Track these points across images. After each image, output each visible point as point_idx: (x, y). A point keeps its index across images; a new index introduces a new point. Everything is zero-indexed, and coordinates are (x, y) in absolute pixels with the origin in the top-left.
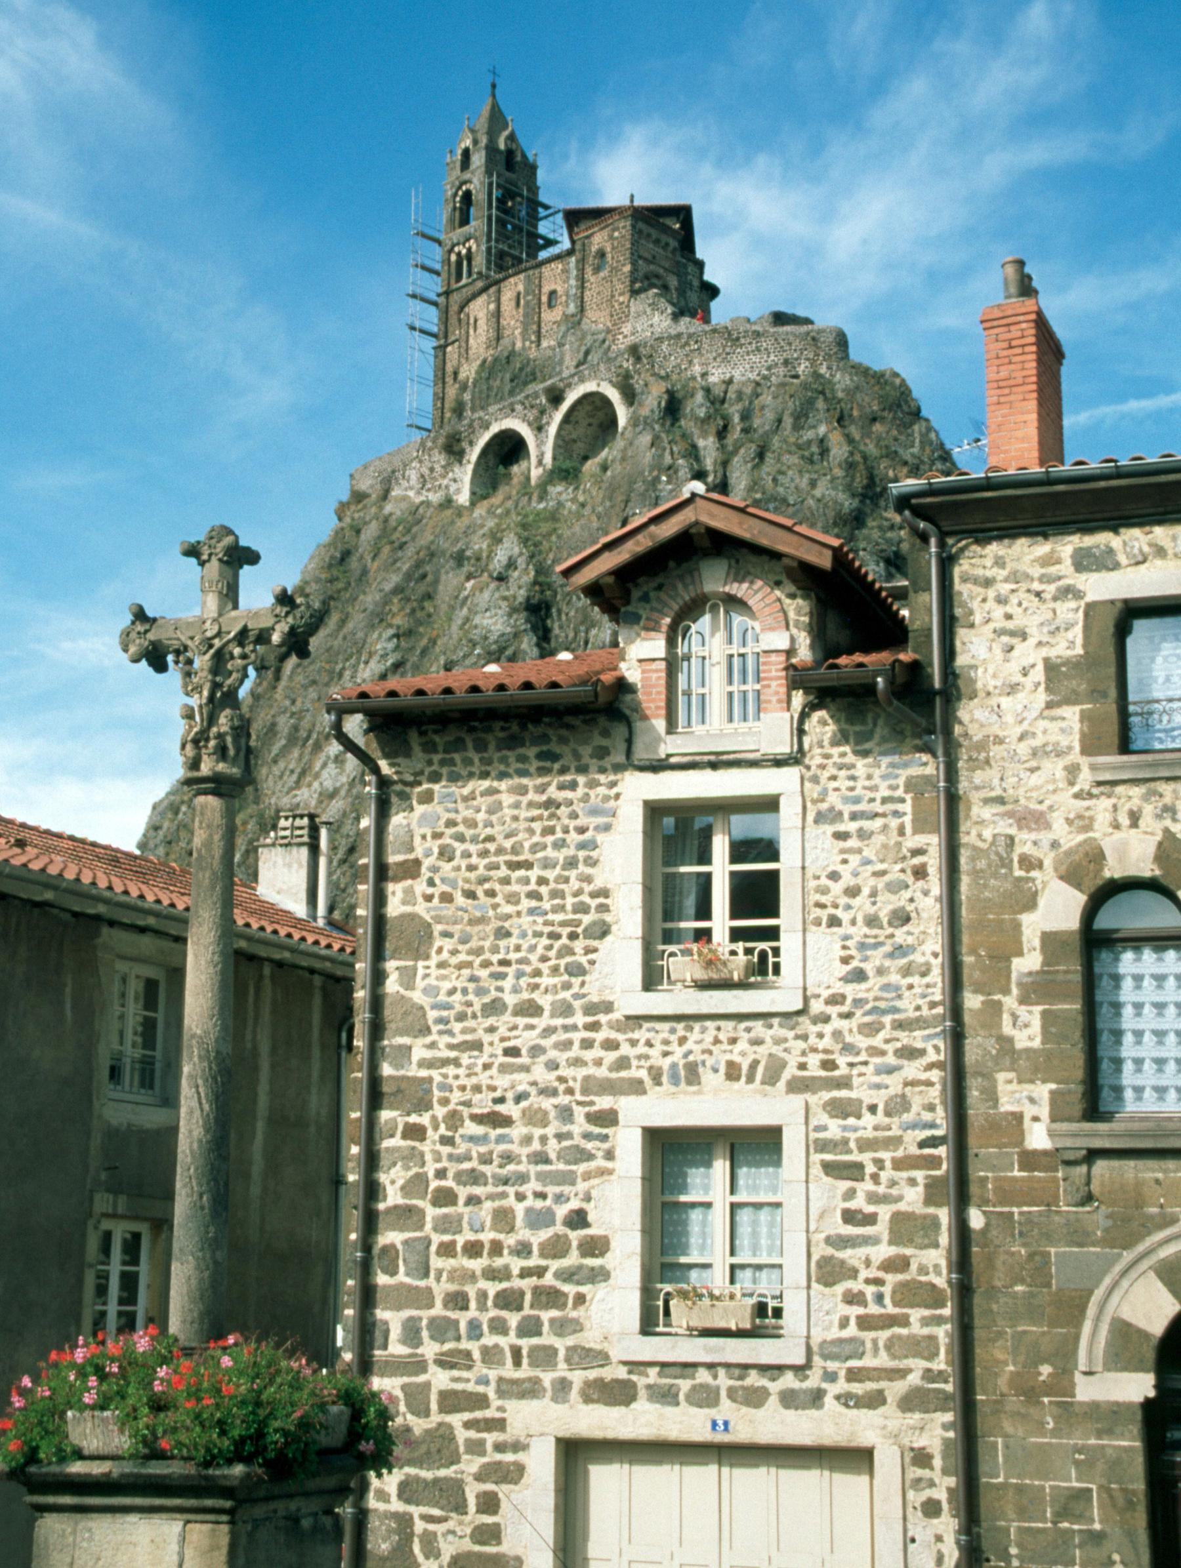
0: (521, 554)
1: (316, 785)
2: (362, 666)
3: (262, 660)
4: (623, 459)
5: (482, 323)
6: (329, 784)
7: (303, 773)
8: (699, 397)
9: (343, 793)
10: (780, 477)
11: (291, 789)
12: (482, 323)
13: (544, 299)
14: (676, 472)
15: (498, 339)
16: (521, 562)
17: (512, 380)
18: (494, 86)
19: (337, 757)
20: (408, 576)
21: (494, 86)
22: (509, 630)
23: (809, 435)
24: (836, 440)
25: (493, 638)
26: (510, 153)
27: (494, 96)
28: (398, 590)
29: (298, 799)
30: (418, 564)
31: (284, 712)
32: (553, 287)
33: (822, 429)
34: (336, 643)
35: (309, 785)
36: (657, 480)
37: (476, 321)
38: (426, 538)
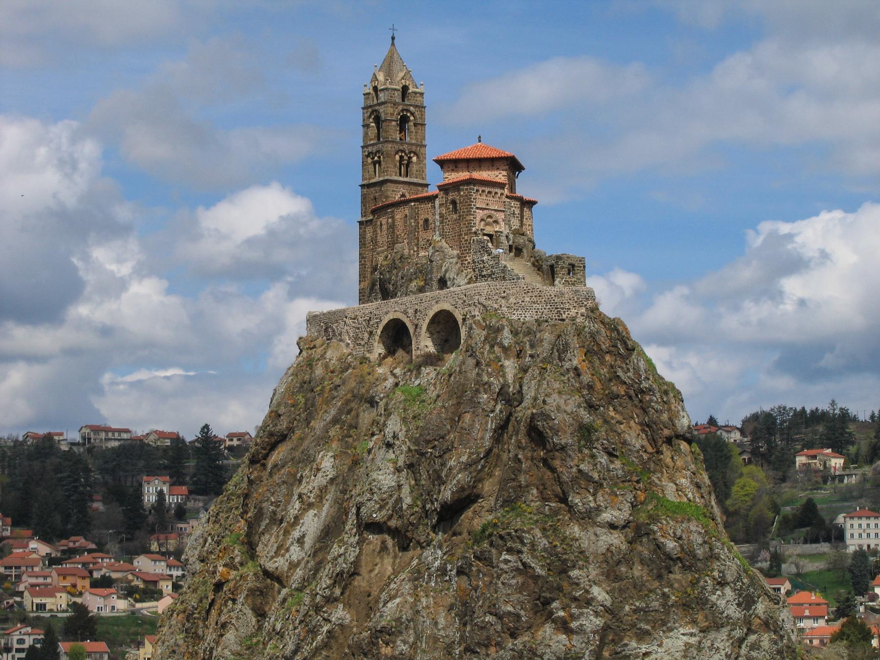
0: (401, 430)
1: (287, 555)
2: (313, 477)
3: (253, 456)
4: (460, 372)
5: (385, 227)
6: (295, 558)
7: (279, 548)
8: (506, 333)
9: (303, 564)
10: (546, 399)
11: (272, 557)
12: (385, 227)
13: (421, 222)
14: (490, 386)
15: (394, 244)
16: (401, 435)
17: (402, 278)
18: (393, 38)
19: (299, 539)
20: (340, 411)
21: (393, 38)
22: (393, 484)
23: (567, 365)
24: (584, 367)
25: (385, 489)
26: (405, 89)
27: (393, 44)
28: (335, 421)
29: (277, 564)
30: (347, 402)
31: (267, 500)
32: (427, 216)
33: (575, 362)
34: (297, 454)
35: (283, 556)
36: (477, 391)
37: (381, 225)
38: (352, 384)
